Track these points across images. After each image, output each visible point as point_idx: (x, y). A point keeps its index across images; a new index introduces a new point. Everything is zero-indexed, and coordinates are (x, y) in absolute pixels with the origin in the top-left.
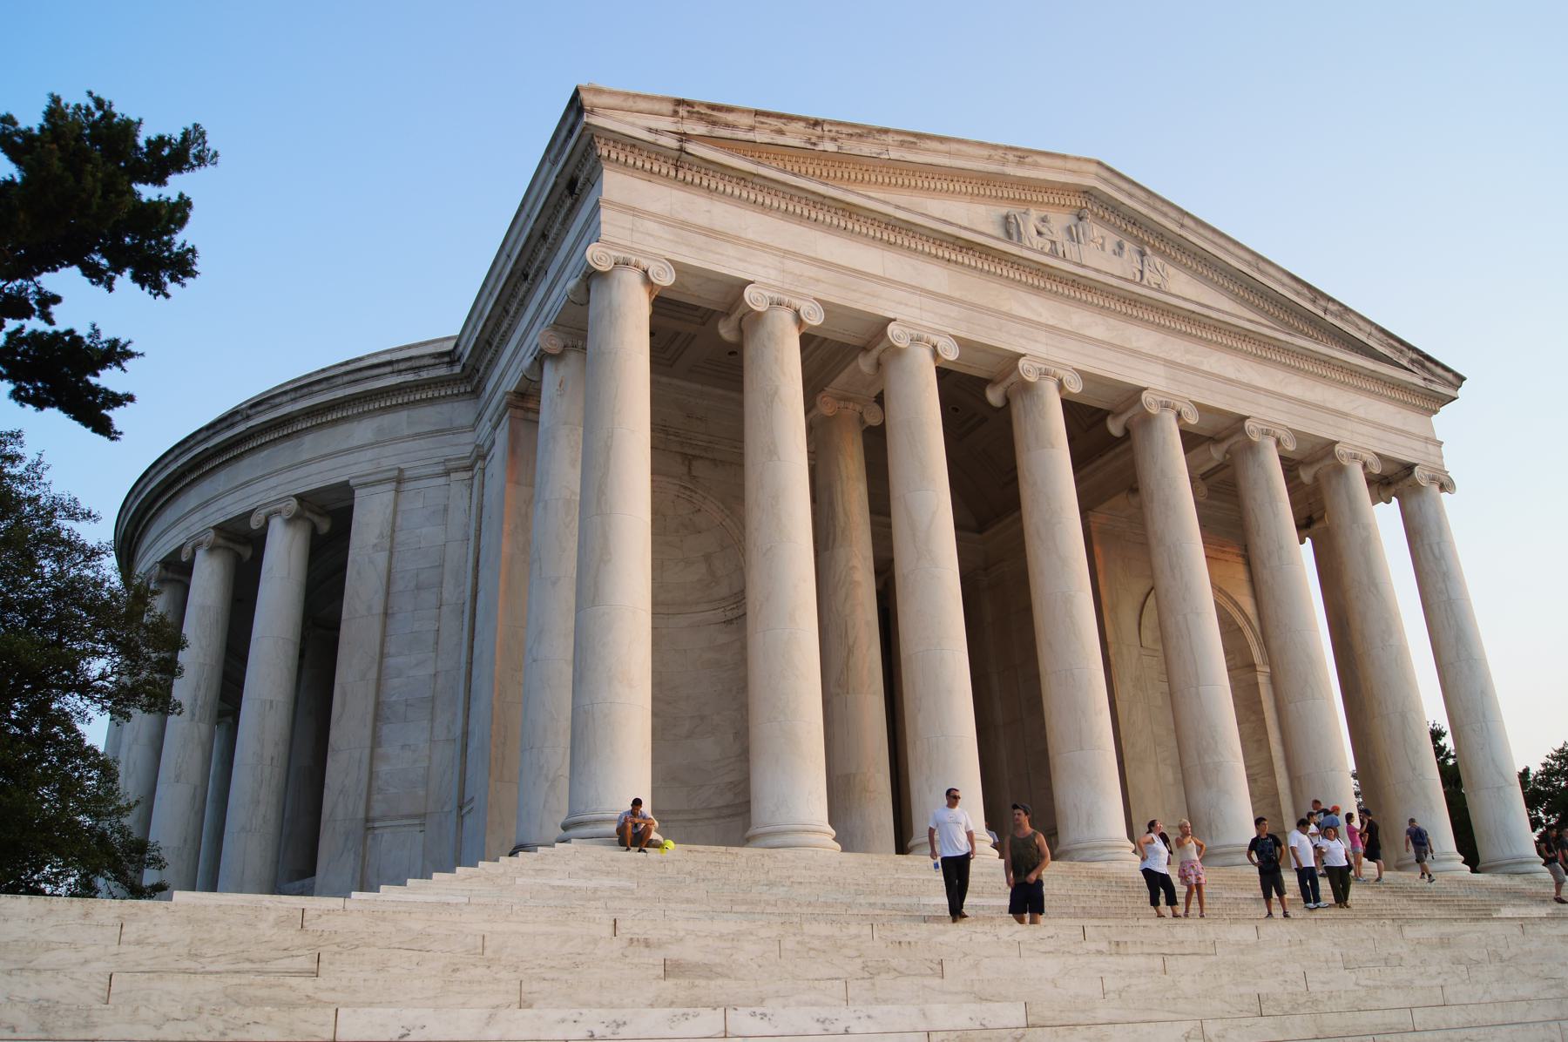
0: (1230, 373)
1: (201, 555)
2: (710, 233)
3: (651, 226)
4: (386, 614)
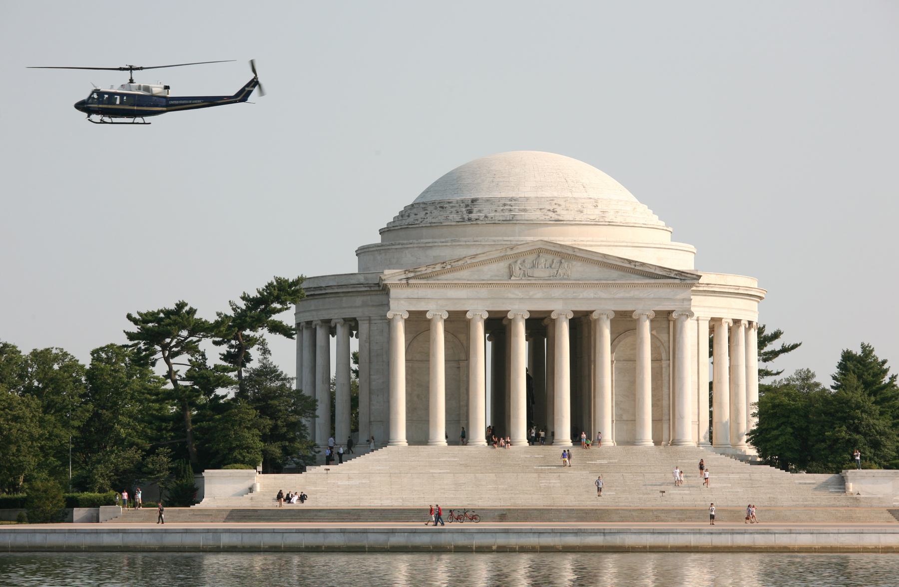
0: (592, 296)
1: (318, 328)
3: (402, 302)
4: (370, 362)
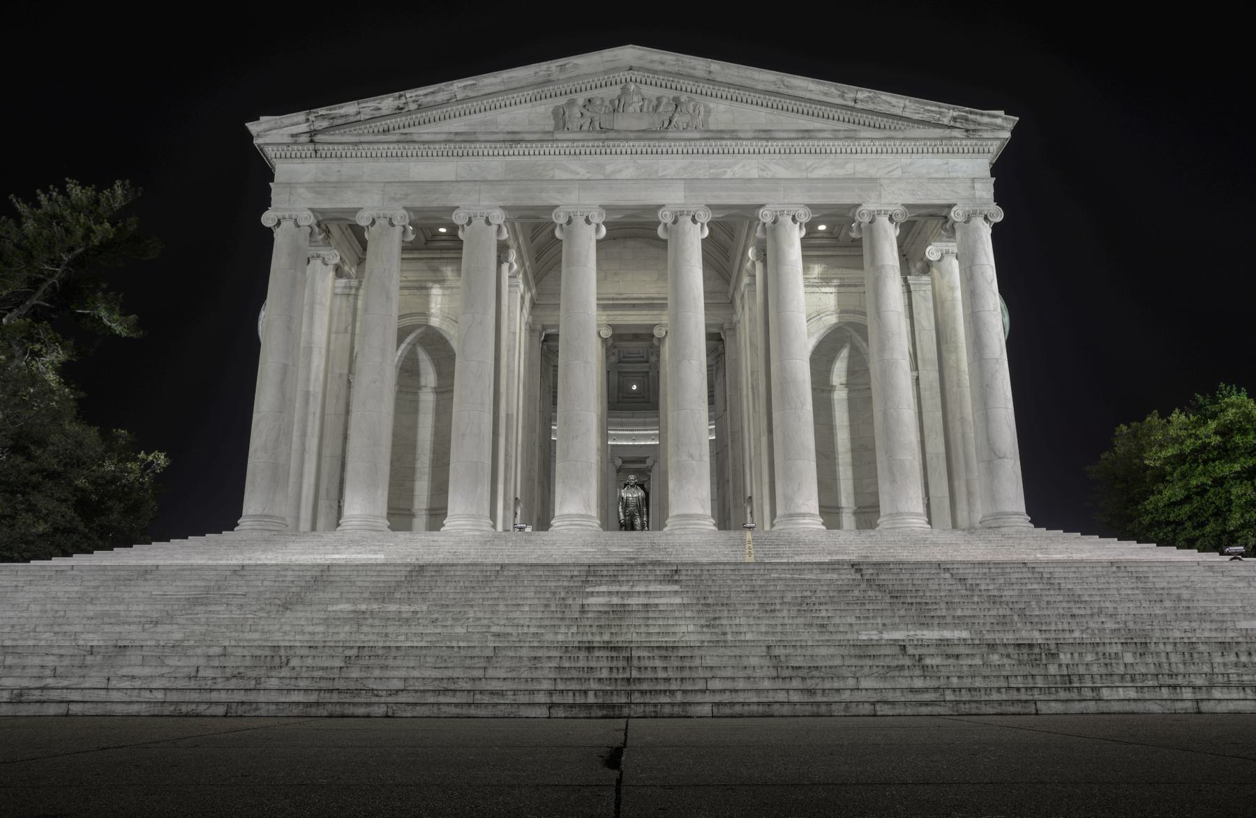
0: (754, 174)
2: (340, 185)
